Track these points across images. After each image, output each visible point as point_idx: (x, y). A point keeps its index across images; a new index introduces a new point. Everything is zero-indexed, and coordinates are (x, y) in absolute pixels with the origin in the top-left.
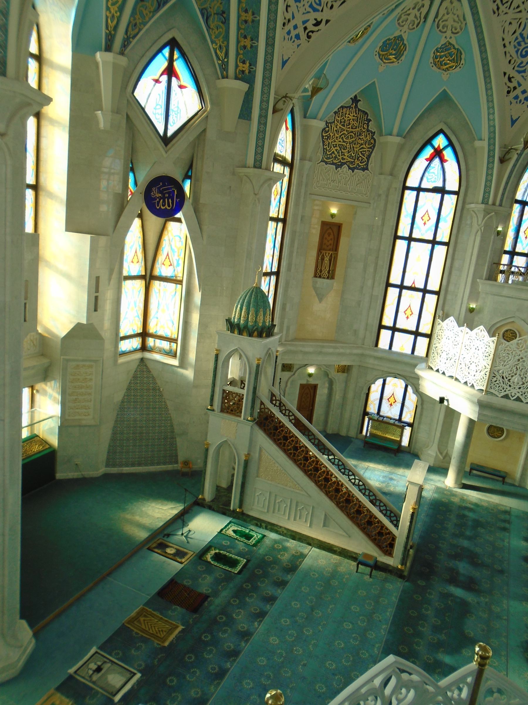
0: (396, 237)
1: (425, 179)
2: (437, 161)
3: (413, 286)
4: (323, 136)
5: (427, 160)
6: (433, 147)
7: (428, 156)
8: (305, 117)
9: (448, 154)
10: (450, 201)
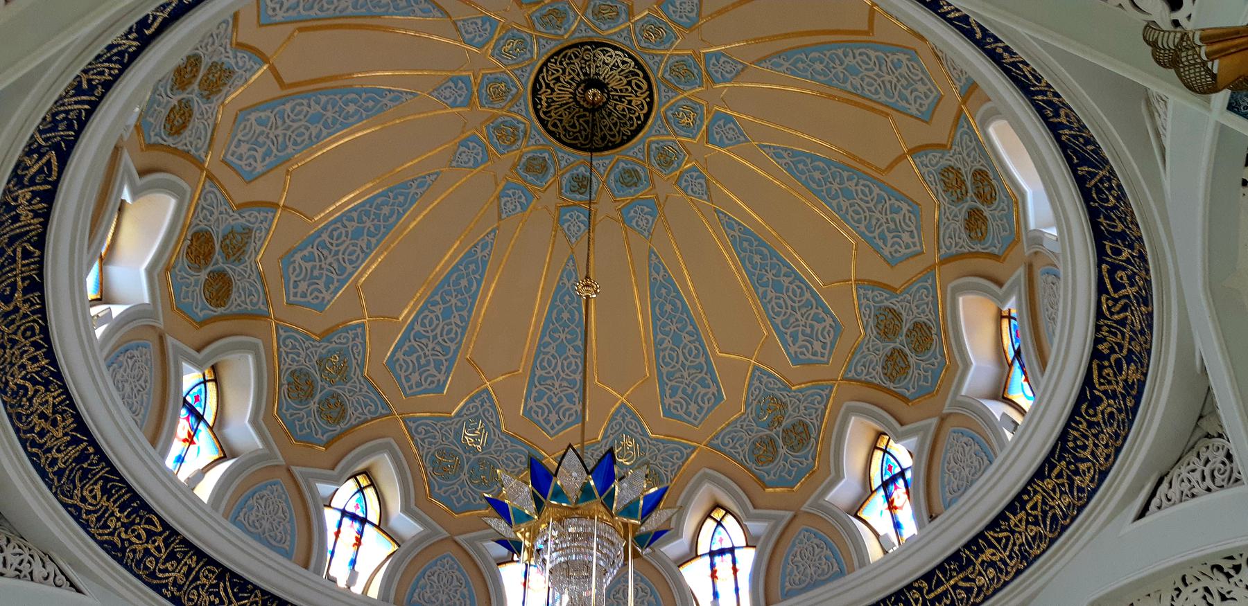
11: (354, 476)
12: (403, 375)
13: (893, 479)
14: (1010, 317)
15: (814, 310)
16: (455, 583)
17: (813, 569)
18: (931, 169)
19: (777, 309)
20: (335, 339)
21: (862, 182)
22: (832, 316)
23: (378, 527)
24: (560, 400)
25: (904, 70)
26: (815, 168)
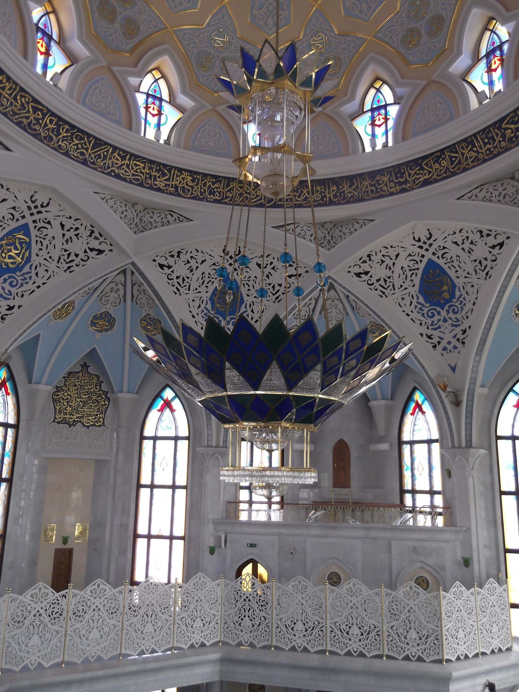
0: (139, 486)
1: (159, 428)
2: (167, 411)
3: (160, 534)
4: (53, 399)
5: (159, 411)
6: (163, 399)
7: (159, 407)
8: (30, 382)
9: (177, 404)
10: (183, 446)
11: (150, 71)
16: (218, 136)
23: (170, 103)
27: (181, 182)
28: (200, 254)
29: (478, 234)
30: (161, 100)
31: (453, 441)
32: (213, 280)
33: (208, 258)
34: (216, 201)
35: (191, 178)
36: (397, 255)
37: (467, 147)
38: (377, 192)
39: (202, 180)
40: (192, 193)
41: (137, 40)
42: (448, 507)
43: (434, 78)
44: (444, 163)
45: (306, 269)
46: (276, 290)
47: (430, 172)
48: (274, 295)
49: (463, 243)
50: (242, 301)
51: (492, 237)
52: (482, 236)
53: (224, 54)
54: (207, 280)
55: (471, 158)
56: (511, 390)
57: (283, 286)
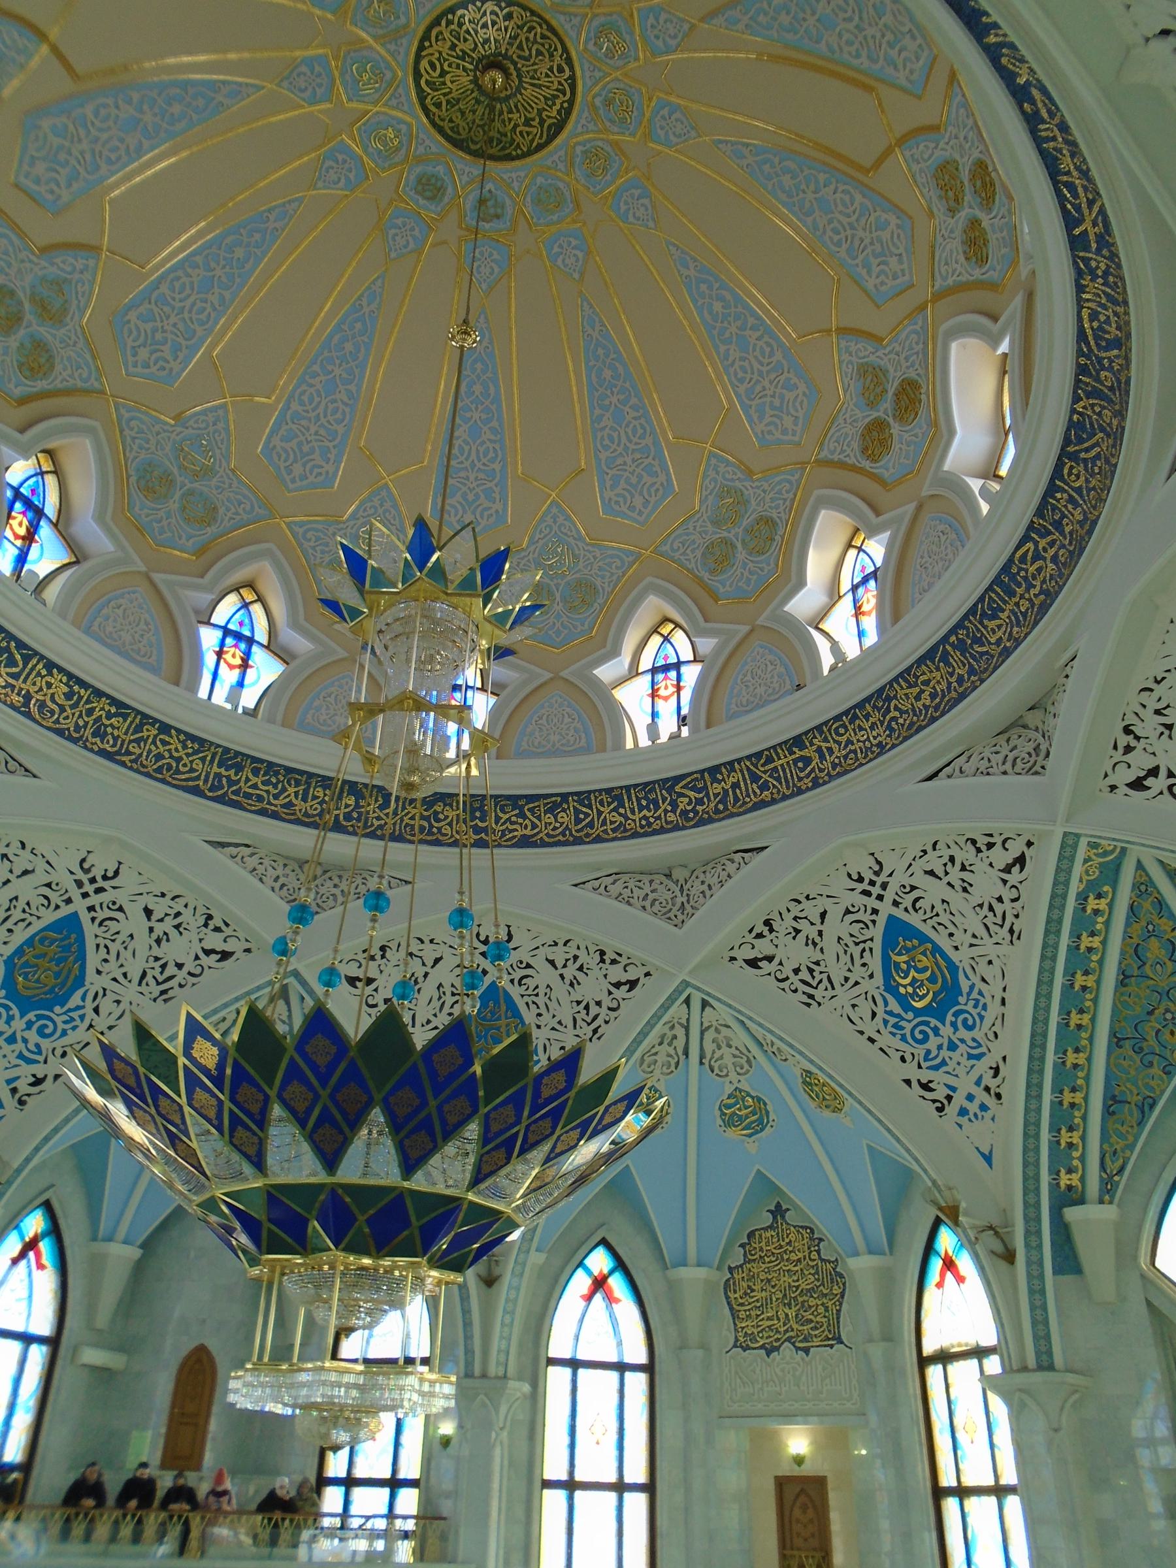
12: (130, 343)
13: (666, 668)
14: (860, 549)
15: (650, 460)
16: (142, 626)
17: (557, 737)
18: (854, 359)
19: (606, 442)
20: (58, 260)
21: (766, 338)
22: (668, 474)
23: (55, 525)
24: (312, 451)
25: (885, 235)
26: (721, 299)
27: (41, 689)
28: (26, 854)
29: (597, 957)
30: (39, 513)
31: (469, 1364)
32: (30, 919)
33: (41, 865)
34: (103, 753)
35: (66, 689)
36: (437, 961)
37: (609, 804)
38: (430, 833)
39: (88, 701)
40: (57, 721)
41: (41, 385)
42: (428, 1515)
43: (564, 674)
44: (563, 817)
45: (248, 945)
46: (167, 974)
47: (534, 826)
48: (158, 983)
49: (565, 966)
50: (80, 981)
51: (620, 967)
52: (603, 961)
53: (196, 485)
54: (17, 914)
55: (612, 823)
56: (581, 1264)
57: (185, 969)
